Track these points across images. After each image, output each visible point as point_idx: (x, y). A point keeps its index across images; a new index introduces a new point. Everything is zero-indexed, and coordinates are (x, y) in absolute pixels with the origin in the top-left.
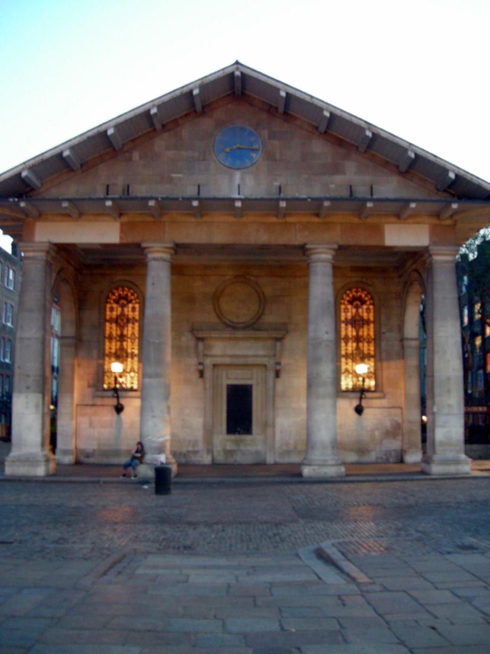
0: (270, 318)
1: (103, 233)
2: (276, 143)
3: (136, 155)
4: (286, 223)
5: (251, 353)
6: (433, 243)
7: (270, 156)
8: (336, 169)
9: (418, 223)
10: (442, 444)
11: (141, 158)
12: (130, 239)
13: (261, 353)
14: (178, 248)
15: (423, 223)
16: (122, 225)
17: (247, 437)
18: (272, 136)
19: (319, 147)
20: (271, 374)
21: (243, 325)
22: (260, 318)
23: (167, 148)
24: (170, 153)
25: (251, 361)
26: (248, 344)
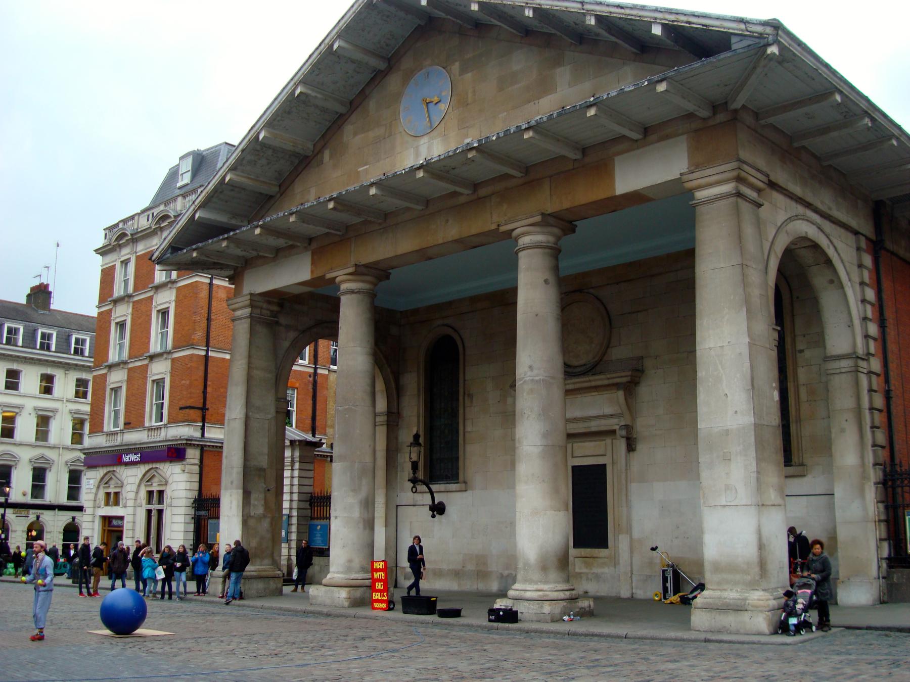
0: (620, 352)
1: (294, 274)
2: (469, 76)
3: (327, 154)
4: (480, 198)
5: (593, 412)
6: (696, 166)
7: (461, 101)
8: (545, 87)
9: (667, 137)
10: (718, 568)
11: (331, 157)
12: (319, 273)
13: (608, 410)
14: (378, 273)
15: (677, 135)
16: (313, 254)
17: (602, 552)
18: (463, 71)
19: (523, 62)
20: (622, 445)
21: (582, 369)
22: (604, 354)
23: (355, 134)
24: (358, 139)
25: (594, 426)
26: (587, 398)
